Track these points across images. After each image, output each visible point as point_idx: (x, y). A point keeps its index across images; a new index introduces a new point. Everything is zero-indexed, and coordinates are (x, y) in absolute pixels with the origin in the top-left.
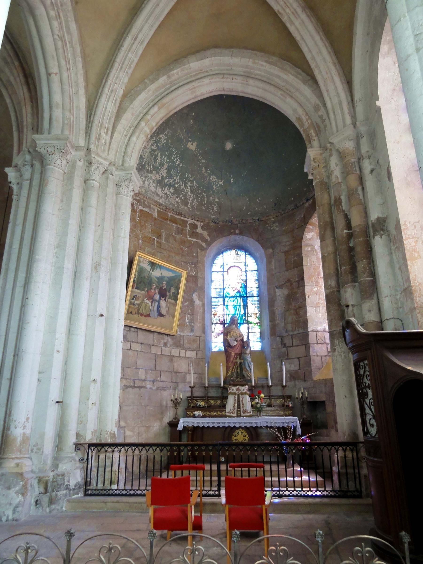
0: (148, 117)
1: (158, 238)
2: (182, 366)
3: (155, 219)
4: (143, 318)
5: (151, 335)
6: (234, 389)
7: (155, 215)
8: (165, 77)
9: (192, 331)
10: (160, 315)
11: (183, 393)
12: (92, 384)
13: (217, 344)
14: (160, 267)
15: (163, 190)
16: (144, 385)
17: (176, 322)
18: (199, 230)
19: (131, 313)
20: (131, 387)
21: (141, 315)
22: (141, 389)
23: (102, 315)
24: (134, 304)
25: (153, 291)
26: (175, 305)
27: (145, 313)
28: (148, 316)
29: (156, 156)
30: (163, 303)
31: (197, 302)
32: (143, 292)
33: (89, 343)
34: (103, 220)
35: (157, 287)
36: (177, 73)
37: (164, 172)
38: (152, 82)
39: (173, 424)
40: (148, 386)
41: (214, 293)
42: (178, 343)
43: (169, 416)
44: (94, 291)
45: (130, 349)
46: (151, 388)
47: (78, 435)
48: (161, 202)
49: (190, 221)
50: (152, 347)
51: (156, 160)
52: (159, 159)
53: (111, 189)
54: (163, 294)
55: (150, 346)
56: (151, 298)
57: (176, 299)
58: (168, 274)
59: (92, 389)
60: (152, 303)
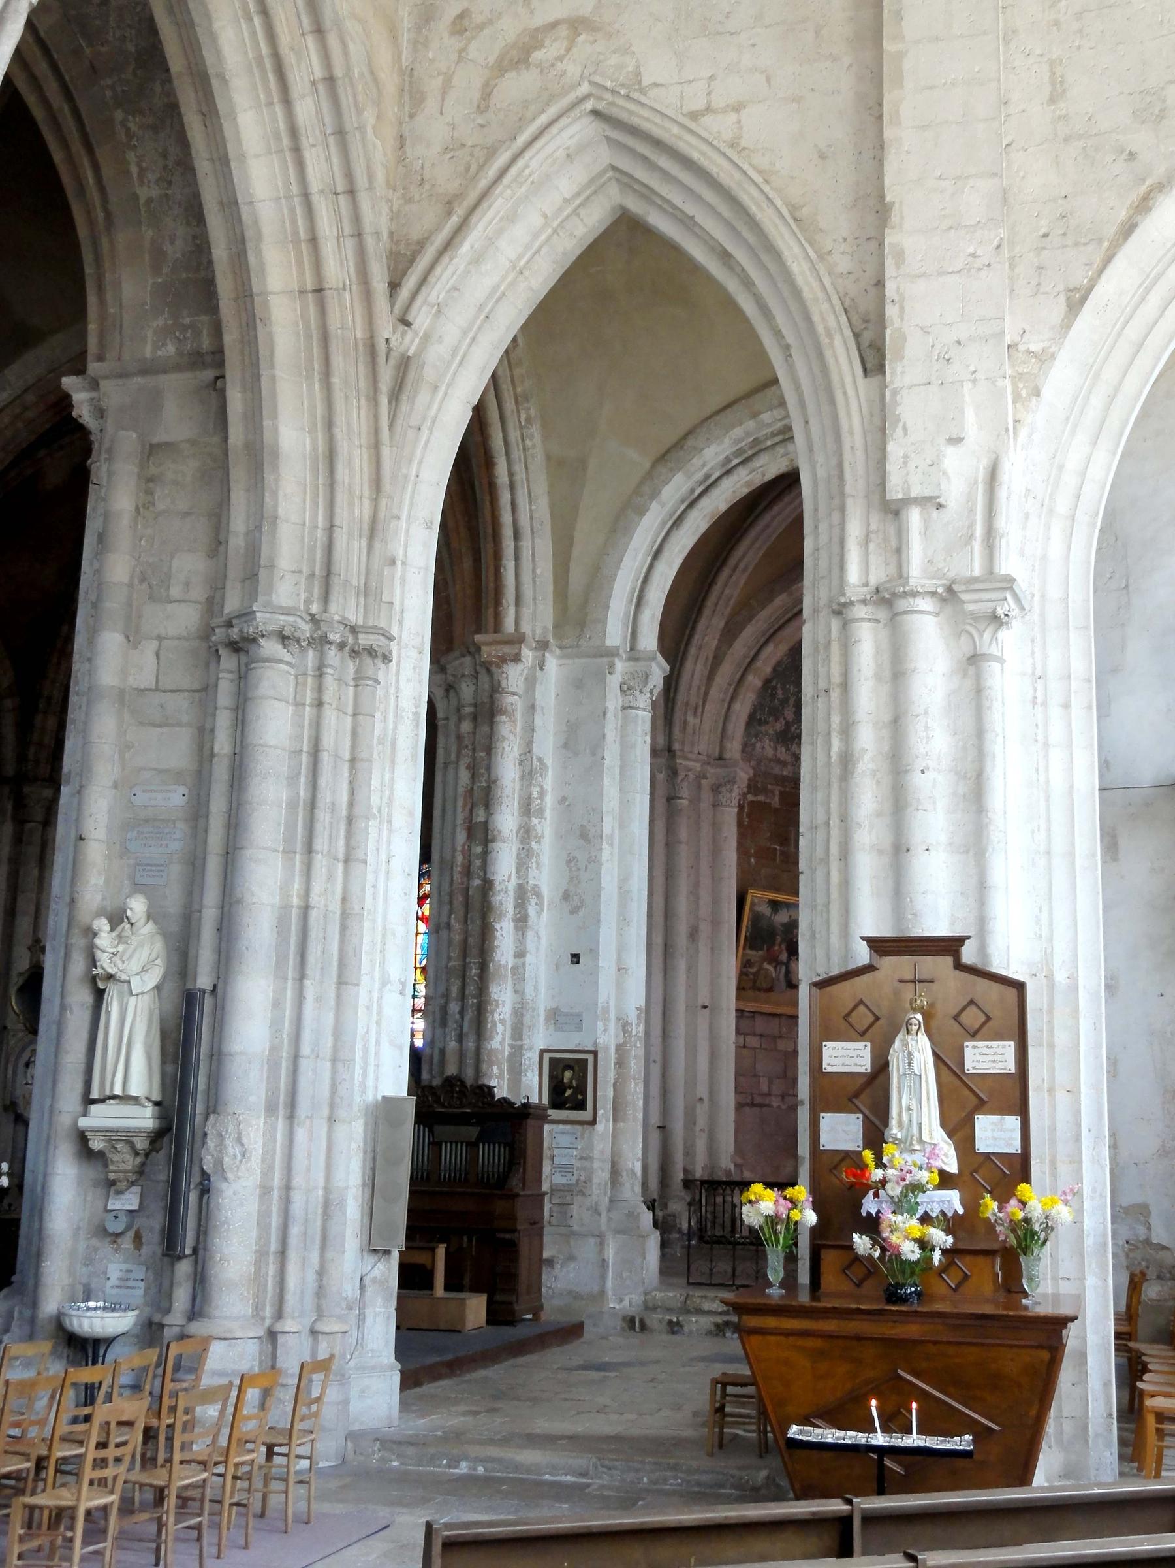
0: (759, 663)
1: (781, 845)
3: (776, 810)
4: (763, 995)
5: (777, 1020)
8: (783, 596)
12: (698, 1105)
15: (788, 749)
16: (767, 1102)
19: (743, 989)
20: (747, 1104)
21: (759, 990)
22: (764, 1109)
23: (705, 1007)
24: (747, 975)
25: (776, 948)
27: (764, 986)
28: (770, 990)
29: (775, 688)
32: (760, 953)
33: (691, 1050)
34: (697, 857)
35: (783, 940)
38: (763, 606)
40: (775, 1104)
44: (691, 969)
45: (744, 1047)
46: (779, 1107)
47: (686, 1171)
48: (785, 773)
50: (779, 1041)
51: (773, 696)
52: (780, 692)
53: (707, 796)
55: (775, 1038)
56: (774, 960)
59: (698, 1111)
60: (775, 968)
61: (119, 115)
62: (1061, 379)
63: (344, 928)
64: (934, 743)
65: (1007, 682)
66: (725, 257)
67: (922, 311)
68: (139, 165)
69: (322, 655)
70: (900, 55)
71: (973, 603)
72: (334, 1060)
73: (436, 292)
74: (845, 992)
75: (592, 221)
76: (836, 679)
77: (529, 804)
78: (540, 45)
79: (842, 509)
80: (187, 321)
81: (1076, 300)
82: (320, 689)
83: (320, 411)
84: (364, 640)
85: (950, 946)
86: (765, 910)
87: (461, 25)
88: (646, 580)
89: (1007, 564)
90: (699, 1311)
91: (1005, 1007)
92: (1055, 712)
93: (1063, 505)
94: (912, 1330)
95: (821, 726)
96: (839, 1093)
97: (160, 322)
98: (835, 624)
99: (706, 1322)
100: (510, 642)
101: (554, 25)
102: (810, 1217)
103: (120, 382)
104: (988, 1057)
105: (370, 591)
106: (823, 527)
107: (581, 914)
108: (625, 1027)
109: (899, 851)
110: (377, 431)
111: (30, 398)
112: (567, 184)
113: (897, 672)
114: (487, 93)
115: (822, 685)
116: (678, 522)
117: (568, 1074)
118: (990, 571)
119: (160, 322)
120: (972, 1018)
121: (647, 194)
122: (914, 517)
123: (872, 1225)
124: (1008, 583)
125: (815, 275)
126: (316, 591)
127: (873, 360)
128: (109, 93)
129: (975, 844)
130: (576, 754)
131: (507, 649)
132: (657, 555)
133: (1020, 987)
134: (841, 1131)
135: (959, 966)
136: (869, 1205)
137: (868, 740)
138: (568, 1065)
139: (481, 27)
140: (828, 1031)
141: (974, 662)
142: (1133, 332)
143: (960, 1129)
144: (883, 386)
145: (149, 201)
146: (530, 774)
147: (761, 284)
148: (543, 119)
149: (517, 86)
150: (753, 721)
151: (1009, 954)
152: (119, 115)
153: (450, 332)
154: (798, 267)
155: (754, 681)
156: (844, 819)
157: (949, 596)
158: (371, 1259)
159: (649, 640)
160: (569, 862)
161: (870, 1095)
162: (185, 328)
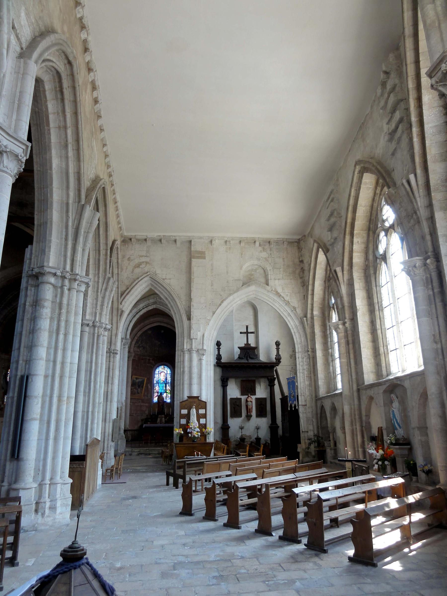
2: (144, 409)
6: (160, 416)
7: (137, 359)
9: (147, 397)
10: (138, 393)
11: (144, 417)
13: (155, 400)
14: (139, 378)
17: (143, 394)
18: (151, 361)
26: (142, 390)
30: (139, 390)
31: (149, 387)
36: (147, 322)
37: (140, 343)
39: (142, 425)
41: (155, 382)
42: (143, 401)
43: (140, 424)
49: (148, 358)
54: (139, 387)
56: (136, 389)
57: (143, 387)
58: (140, 380)
62: (211, 323)
63: (111, 394)
64: (195, 370)
65: (204, 362)
66: (166, 299)
67: (195, 313)
69: (110, 354)
70: (194, 278)
71: (201, 352)
72: (110, 413)
73: (125, 300)
74: (184, 403)
75: (147, 289)
76: (182, 360)
78: (141, 265)
79: (184, 338)
81: (214, 313)
82: (110, 359)
83: (111, 318)
84: (115, 352)
85: (197, 397)
86: (135, 379)
87: (129, 259)
88: (128, 326)
89: (205, 348)
90: (134, 452)
91: (203, 405)
92: (209, 366)
93: (210, 339)
94: (196, 445)
95: (179, 366)
96: (182, 416)
98: (182, 353)
99: (136, 453)
101: (143, 262)
102: (183, 432)
104: (202, 411)
105: (115, 344)
106: (180, 339)
108: (122, 404)
109: (190, 384)
110: (117, 321)
112: (144, 286)
113: (191, 360)
114: (133, 271)
115: (179, 361)
116: (135, 316)
118: (203, 348)
120: (200, 407)
121: (156, 288)
122: (194, 340)
123: (189, 433)
124: (205, 350)
125: (181, 304)
126: (109, 345)
127: (189, 319)
129: (200, 384)
132: (131, 322)
133: (206, 402)
134: (183, 421)
135: (199, 400)
136: (188, 430)
137: (186, 369)
139: (132, 260)
140: (182, 408)
141: (200, 360)
142: (220, 317)
143: (198, 420)
144: (190, 323)
147: (172, 303)
148: (143, 277)
149: (137, 270)
150: (135, 344)
151: (204, 398)
153: (126, 305)
154: (179, 304)
155: (136, 338)
156: (183, 379)
157: (198, 351)
158: (112, 442)
159: (128, 336)
161: (188, 417)
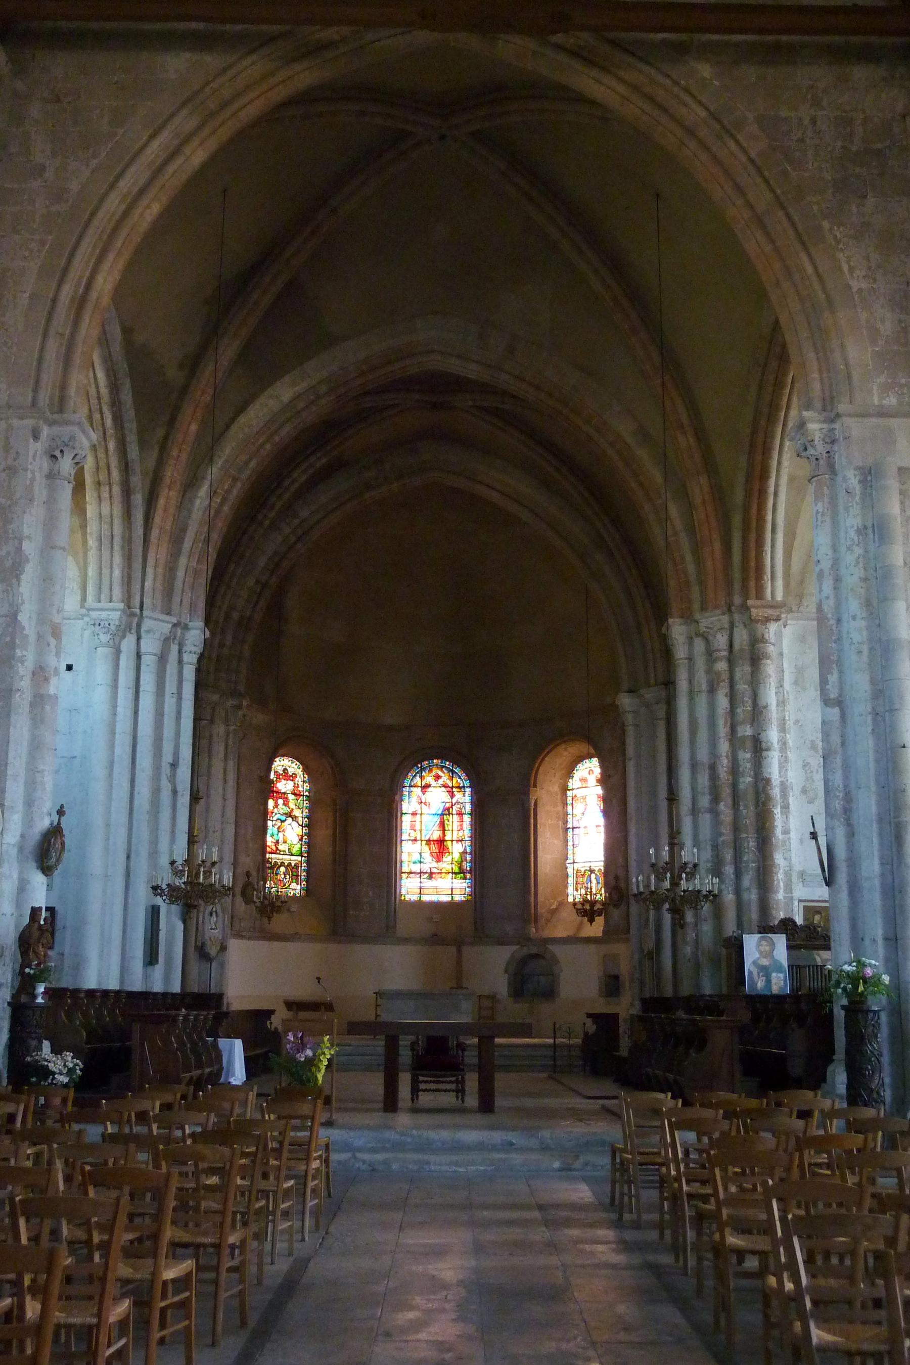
61: (826, 224)
68: (848, 262)
77: (784, 724)
80: (903, 381)
97: (882, 379)
100: (774, 606)
103: (860, 420)
107: (816, 803)
111: (323, 389)
117: (817, 918)
119: (882, 379)
128: (815, 207)
130: (804, 689)
131: (770, 612)
138: (817, 910)
145: (860, 290)
146: (783, 702)
152: (826, 224)
160: (804, 766)
162: (902, 386)
